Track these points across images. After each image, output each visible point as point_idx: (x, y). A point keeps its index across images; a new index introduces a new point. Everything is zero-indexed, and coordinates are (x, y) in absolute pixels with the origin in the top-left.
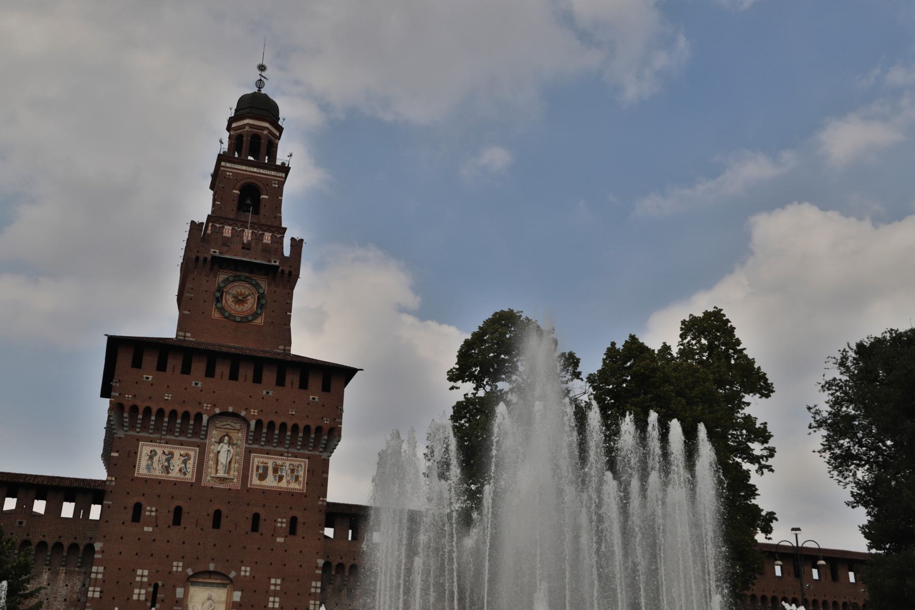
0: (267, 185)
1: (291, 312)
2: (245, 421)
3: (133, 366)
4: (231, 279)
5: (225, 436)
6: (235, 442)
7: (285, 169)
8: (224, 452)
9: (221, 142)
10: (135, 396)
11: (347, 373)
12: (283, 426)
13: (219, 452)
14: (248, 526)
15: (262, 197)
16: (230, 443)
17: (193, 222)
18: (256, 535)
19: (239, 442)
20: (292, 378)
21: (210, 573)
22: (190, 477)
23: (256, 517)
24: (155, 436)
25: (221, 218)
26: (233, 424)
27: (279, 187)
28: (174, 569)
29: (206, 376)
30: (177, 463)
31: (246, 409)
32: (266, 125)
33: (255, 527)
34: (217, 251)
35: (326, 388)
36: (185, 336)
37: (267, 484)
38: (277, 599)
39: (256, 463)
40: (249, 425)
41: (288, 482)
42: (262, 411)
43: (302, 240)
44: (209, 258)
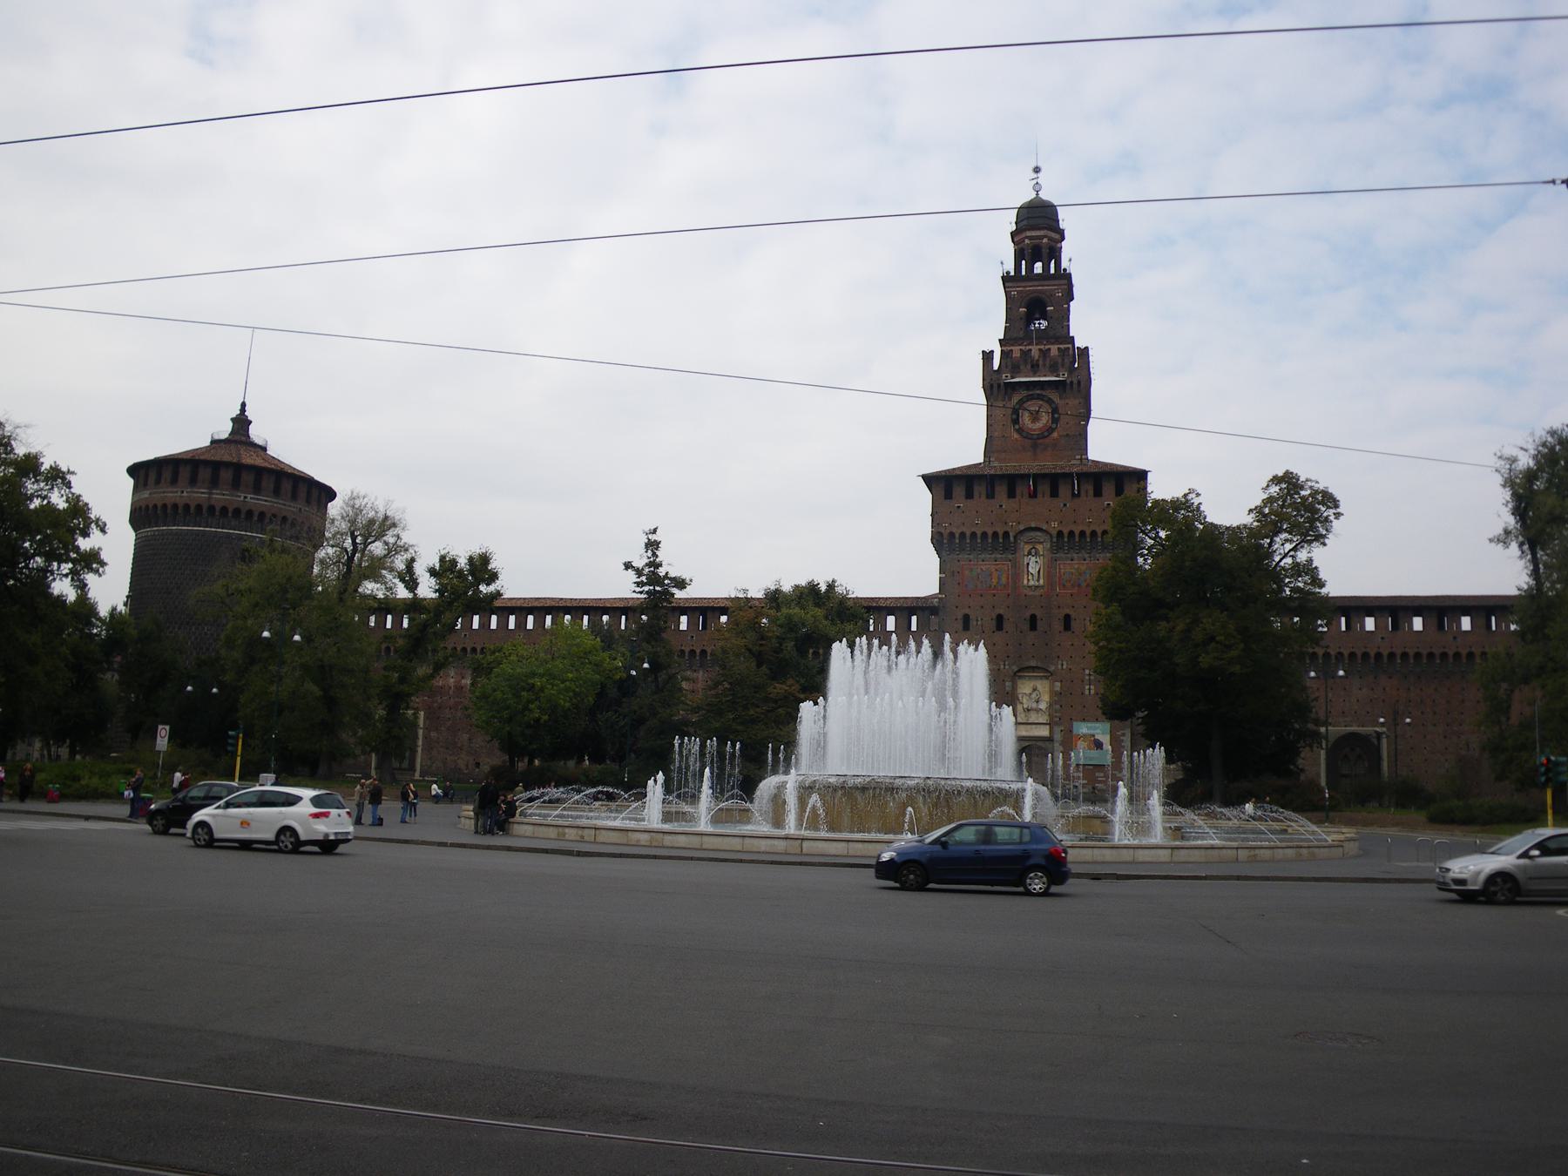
4: (1025, 400)
9: (1002, 263)
12: (1082, 533)
13: (1028, 564)
14: (1058, 626)
15: (1048, 308)
17: (983, 352)
21: (1033, 669)
23: (1067, 619)
35: (1119, 491)
38: (1092, 687)
43: (1087, 348)
44: (1002, 384)
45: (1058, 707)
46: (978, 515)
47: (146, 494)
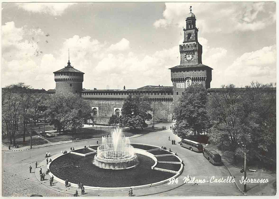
2: (191, 79)
30: (182, 85)
46: (179, 75)
47: (56, 77)
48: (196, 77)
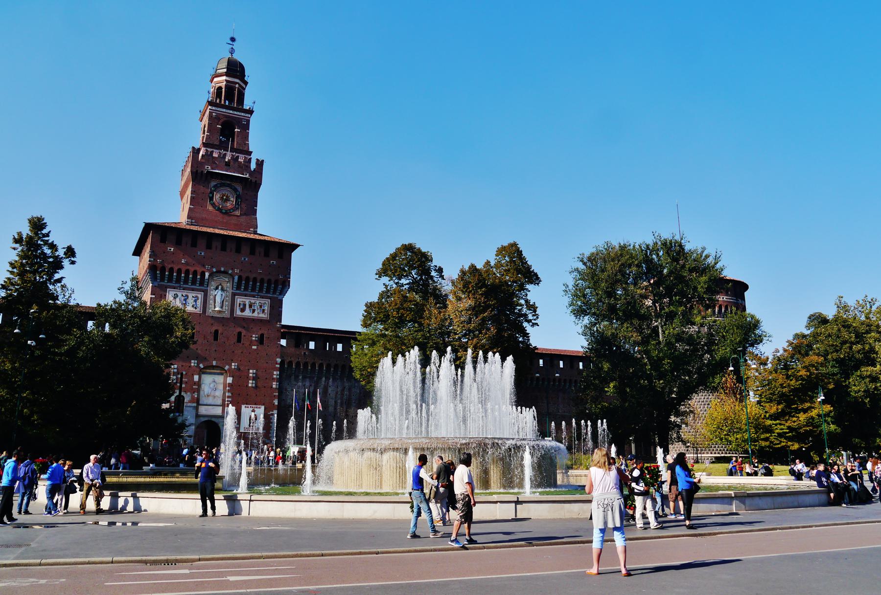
0: (239, 122)
1: (256, 207)
3: (162, 242)
5: (219, 285)
6: (225, 289)
7: (251, 112)
8: (219, 295)
10: (163, 261)
11: (295, 247)
13: (216, 295)
14: (236, 340)
15: (236, 130)
16: (222, 290)
18: (240, 345)
19: (228, 289)
20: (260, 250)
21: (213, 367)
22: (198, 310)
24: (177, 285)
25: (210, 144)
26: (224, 278)
27: (247, 124)
28: (192, 364)
29: (207, 248)
30: (191, 301)
31: (232, 269)
32: (237, 81)
33: (239, 340)
34: (210, 167)
35: (280, 256)
36: (191, 222)
37: (245, 315)
39: (238, 302)
40: (233, 279)
41: (258, 313)
42: (242, 270)
43: (263, 161)
45: (230, 394)
48: (254, 276)
